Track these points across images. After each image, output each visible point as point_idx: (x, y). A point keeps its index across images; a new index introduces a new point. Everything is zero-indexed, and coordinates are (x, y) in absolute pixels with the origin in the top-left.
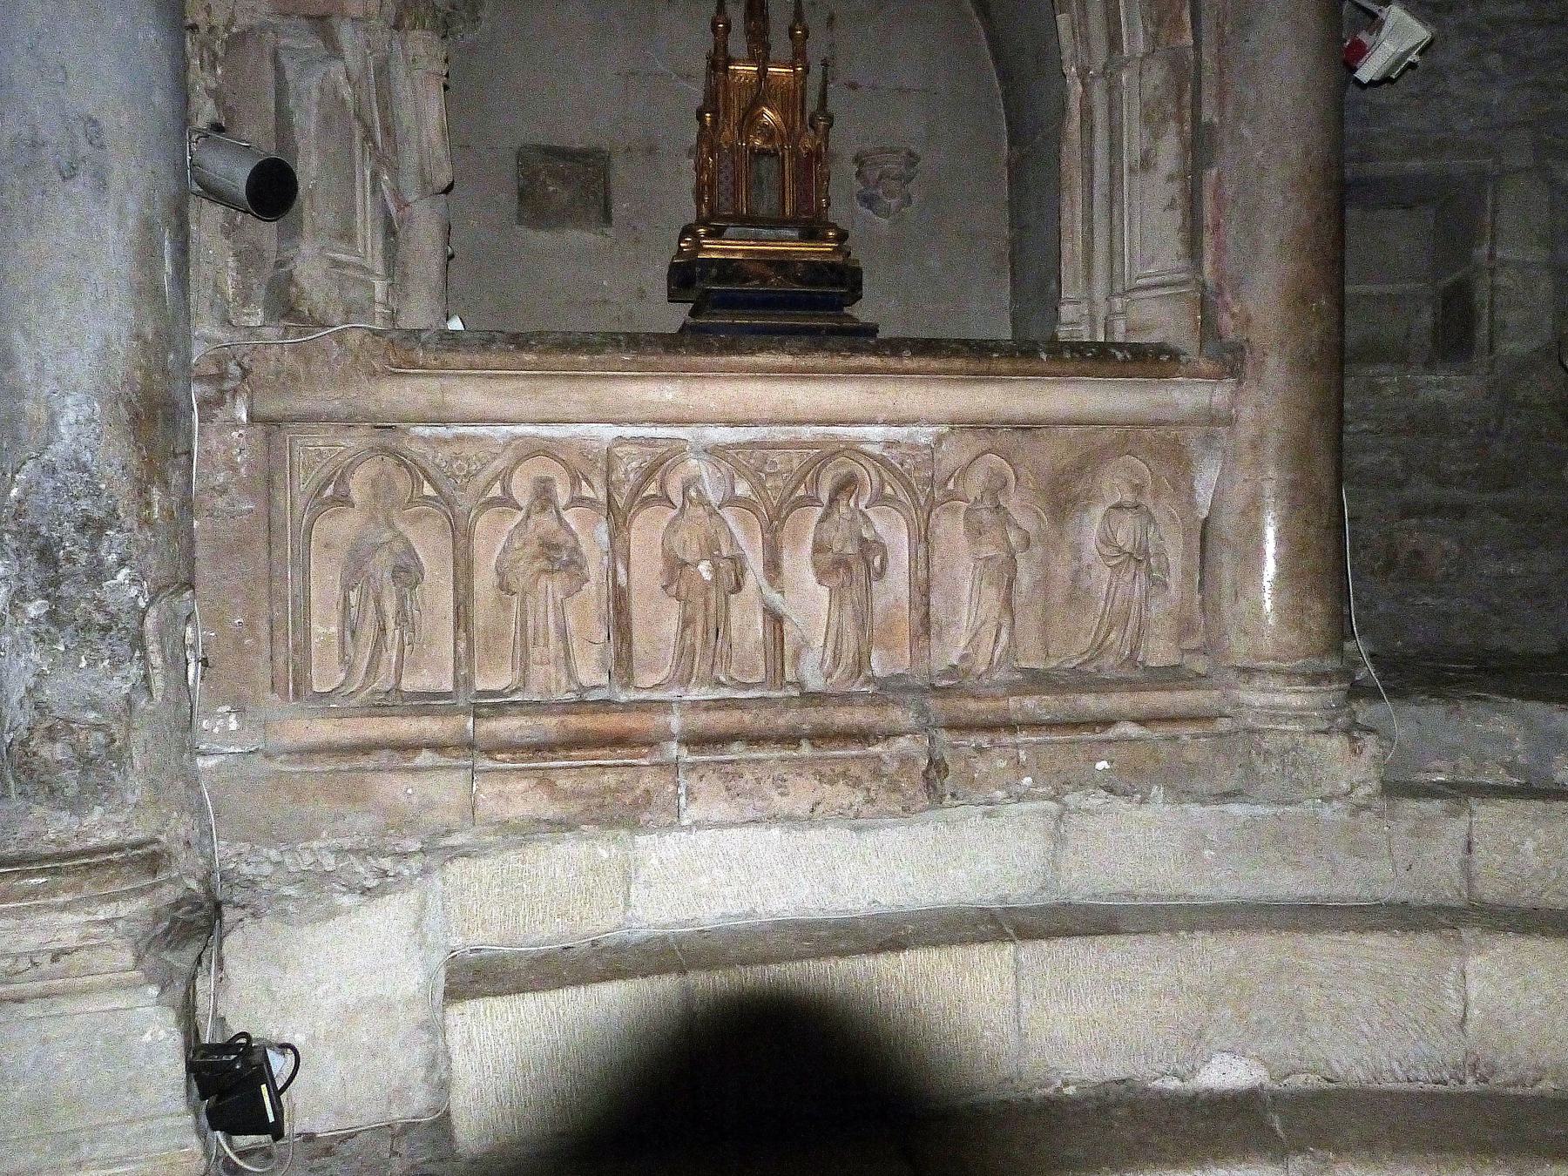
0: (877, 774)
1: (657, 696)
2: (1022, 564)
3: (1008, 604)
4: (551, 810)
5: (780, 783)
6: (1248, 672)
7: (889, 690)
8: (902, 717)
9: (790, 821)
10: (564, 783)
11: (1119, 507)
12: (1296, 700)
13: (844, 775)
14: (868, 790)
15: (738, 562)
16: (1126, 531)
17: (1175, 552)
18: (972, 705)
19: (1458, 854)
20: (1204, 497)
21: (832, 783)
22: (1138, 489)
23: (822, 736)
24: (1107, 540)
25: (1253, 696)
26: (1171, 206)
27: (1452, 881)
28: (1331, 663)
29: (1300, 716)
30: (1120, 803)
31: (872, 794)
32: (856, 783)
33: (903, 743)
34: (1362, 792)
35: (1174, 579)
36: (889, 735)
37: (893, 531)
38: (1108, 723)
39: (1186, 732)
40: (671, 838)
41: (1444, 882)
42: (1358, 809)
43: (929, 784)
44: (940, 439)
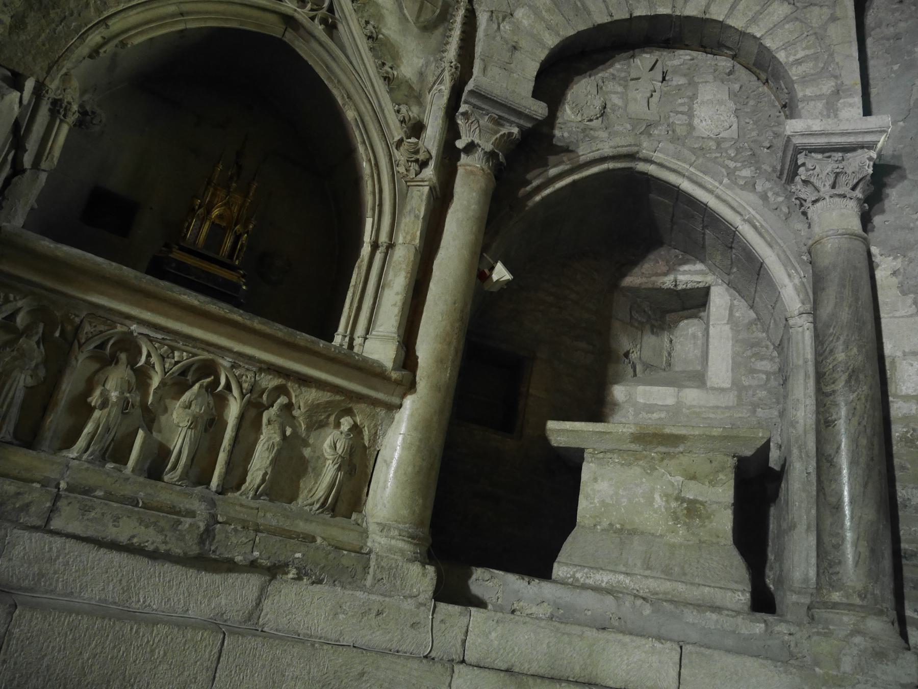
13: (155, 524)
14: (166, 536)
19: (461, 637)
21: (147, 527)
26: (395, 305)
27: (456, 651)
29: (402, 552)
31: (168, 539)
32: (161, 531)
41: (453, 650)
42: (421, 604)
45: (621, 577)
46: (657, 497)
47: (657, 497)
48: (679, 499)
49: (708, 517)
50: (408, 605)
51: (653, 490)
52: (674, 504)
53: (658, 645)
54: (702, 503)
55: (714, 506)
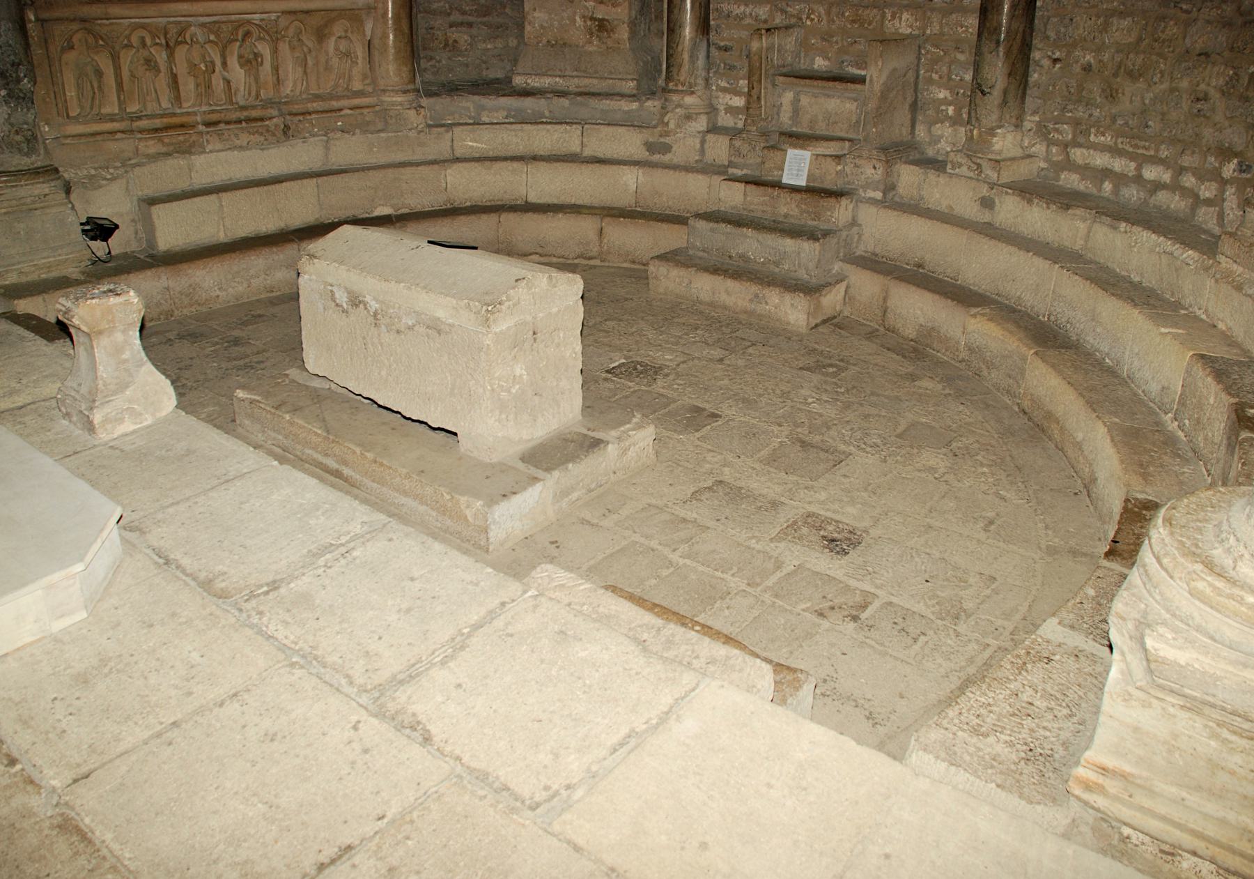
0: (268, 131)
1: (190, 110)
2: (308, 58)
3: (305, 72)
4: (164, 150)
5: (237, 136)
6: (384, 91)
7: (269, 103)
8: (275, 112)
9: (241, 148)
10: (166, 140)
11: (340, 37)
12: (399, 99)
15: (213, 63)
16: (343, 46)
17: (360, 52)
18: (296, 107)
19: (449, 144)
20: (368, 33)
22: (346, 31)
23: (248, 120)
24: (336, 49)
25: (387, 98)
28: (411, 87)
30: (346, 135)
32: (261, 134)
33: (275, 120)
34: (421, 126)
35: (360, 61)
36: (270, 118)
37: (264, 49)
38: (341, 110)
39: (365, 111)
40: (202, 156)
43: (285, 133)
44: (278, 17)
45: (557, 79)
46: (578, 19)
47: (578, 19)
48: (592, 19)
49: (612, 30)
50: (413, 134)
51: (575, 13)
52: (589, 23)
53: (568, 127)
54: (607, 20)
55: (616, 22)
